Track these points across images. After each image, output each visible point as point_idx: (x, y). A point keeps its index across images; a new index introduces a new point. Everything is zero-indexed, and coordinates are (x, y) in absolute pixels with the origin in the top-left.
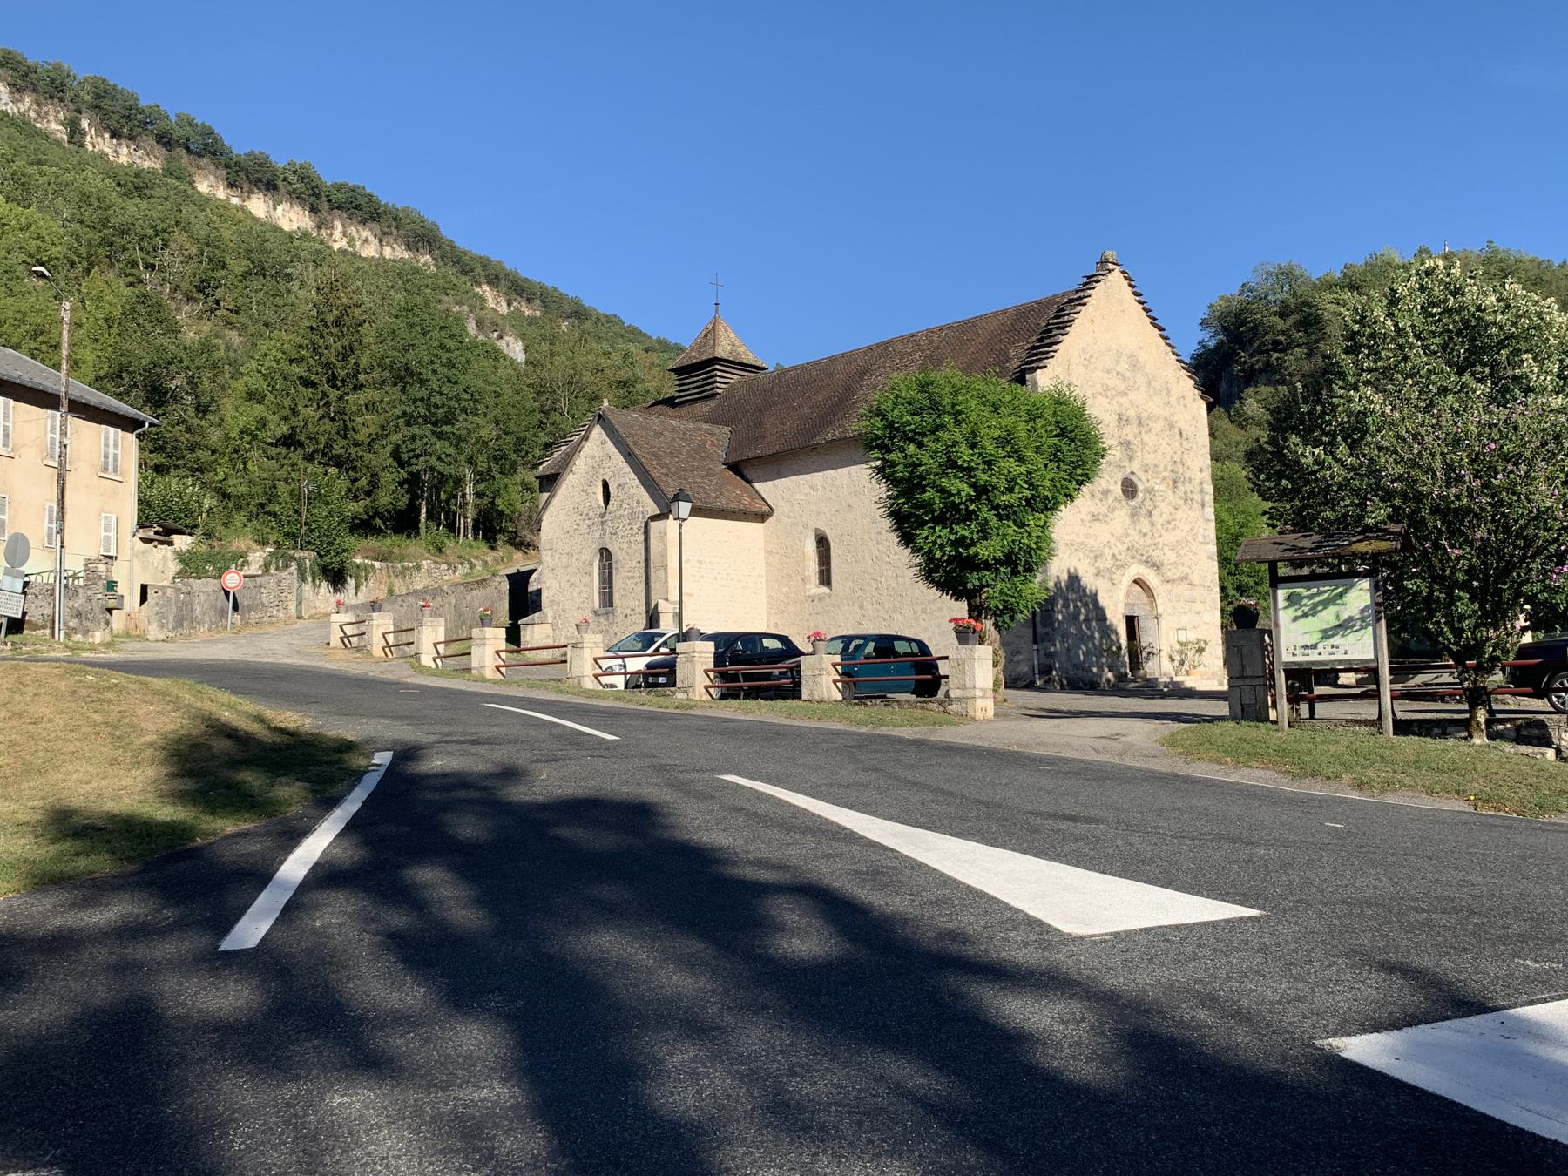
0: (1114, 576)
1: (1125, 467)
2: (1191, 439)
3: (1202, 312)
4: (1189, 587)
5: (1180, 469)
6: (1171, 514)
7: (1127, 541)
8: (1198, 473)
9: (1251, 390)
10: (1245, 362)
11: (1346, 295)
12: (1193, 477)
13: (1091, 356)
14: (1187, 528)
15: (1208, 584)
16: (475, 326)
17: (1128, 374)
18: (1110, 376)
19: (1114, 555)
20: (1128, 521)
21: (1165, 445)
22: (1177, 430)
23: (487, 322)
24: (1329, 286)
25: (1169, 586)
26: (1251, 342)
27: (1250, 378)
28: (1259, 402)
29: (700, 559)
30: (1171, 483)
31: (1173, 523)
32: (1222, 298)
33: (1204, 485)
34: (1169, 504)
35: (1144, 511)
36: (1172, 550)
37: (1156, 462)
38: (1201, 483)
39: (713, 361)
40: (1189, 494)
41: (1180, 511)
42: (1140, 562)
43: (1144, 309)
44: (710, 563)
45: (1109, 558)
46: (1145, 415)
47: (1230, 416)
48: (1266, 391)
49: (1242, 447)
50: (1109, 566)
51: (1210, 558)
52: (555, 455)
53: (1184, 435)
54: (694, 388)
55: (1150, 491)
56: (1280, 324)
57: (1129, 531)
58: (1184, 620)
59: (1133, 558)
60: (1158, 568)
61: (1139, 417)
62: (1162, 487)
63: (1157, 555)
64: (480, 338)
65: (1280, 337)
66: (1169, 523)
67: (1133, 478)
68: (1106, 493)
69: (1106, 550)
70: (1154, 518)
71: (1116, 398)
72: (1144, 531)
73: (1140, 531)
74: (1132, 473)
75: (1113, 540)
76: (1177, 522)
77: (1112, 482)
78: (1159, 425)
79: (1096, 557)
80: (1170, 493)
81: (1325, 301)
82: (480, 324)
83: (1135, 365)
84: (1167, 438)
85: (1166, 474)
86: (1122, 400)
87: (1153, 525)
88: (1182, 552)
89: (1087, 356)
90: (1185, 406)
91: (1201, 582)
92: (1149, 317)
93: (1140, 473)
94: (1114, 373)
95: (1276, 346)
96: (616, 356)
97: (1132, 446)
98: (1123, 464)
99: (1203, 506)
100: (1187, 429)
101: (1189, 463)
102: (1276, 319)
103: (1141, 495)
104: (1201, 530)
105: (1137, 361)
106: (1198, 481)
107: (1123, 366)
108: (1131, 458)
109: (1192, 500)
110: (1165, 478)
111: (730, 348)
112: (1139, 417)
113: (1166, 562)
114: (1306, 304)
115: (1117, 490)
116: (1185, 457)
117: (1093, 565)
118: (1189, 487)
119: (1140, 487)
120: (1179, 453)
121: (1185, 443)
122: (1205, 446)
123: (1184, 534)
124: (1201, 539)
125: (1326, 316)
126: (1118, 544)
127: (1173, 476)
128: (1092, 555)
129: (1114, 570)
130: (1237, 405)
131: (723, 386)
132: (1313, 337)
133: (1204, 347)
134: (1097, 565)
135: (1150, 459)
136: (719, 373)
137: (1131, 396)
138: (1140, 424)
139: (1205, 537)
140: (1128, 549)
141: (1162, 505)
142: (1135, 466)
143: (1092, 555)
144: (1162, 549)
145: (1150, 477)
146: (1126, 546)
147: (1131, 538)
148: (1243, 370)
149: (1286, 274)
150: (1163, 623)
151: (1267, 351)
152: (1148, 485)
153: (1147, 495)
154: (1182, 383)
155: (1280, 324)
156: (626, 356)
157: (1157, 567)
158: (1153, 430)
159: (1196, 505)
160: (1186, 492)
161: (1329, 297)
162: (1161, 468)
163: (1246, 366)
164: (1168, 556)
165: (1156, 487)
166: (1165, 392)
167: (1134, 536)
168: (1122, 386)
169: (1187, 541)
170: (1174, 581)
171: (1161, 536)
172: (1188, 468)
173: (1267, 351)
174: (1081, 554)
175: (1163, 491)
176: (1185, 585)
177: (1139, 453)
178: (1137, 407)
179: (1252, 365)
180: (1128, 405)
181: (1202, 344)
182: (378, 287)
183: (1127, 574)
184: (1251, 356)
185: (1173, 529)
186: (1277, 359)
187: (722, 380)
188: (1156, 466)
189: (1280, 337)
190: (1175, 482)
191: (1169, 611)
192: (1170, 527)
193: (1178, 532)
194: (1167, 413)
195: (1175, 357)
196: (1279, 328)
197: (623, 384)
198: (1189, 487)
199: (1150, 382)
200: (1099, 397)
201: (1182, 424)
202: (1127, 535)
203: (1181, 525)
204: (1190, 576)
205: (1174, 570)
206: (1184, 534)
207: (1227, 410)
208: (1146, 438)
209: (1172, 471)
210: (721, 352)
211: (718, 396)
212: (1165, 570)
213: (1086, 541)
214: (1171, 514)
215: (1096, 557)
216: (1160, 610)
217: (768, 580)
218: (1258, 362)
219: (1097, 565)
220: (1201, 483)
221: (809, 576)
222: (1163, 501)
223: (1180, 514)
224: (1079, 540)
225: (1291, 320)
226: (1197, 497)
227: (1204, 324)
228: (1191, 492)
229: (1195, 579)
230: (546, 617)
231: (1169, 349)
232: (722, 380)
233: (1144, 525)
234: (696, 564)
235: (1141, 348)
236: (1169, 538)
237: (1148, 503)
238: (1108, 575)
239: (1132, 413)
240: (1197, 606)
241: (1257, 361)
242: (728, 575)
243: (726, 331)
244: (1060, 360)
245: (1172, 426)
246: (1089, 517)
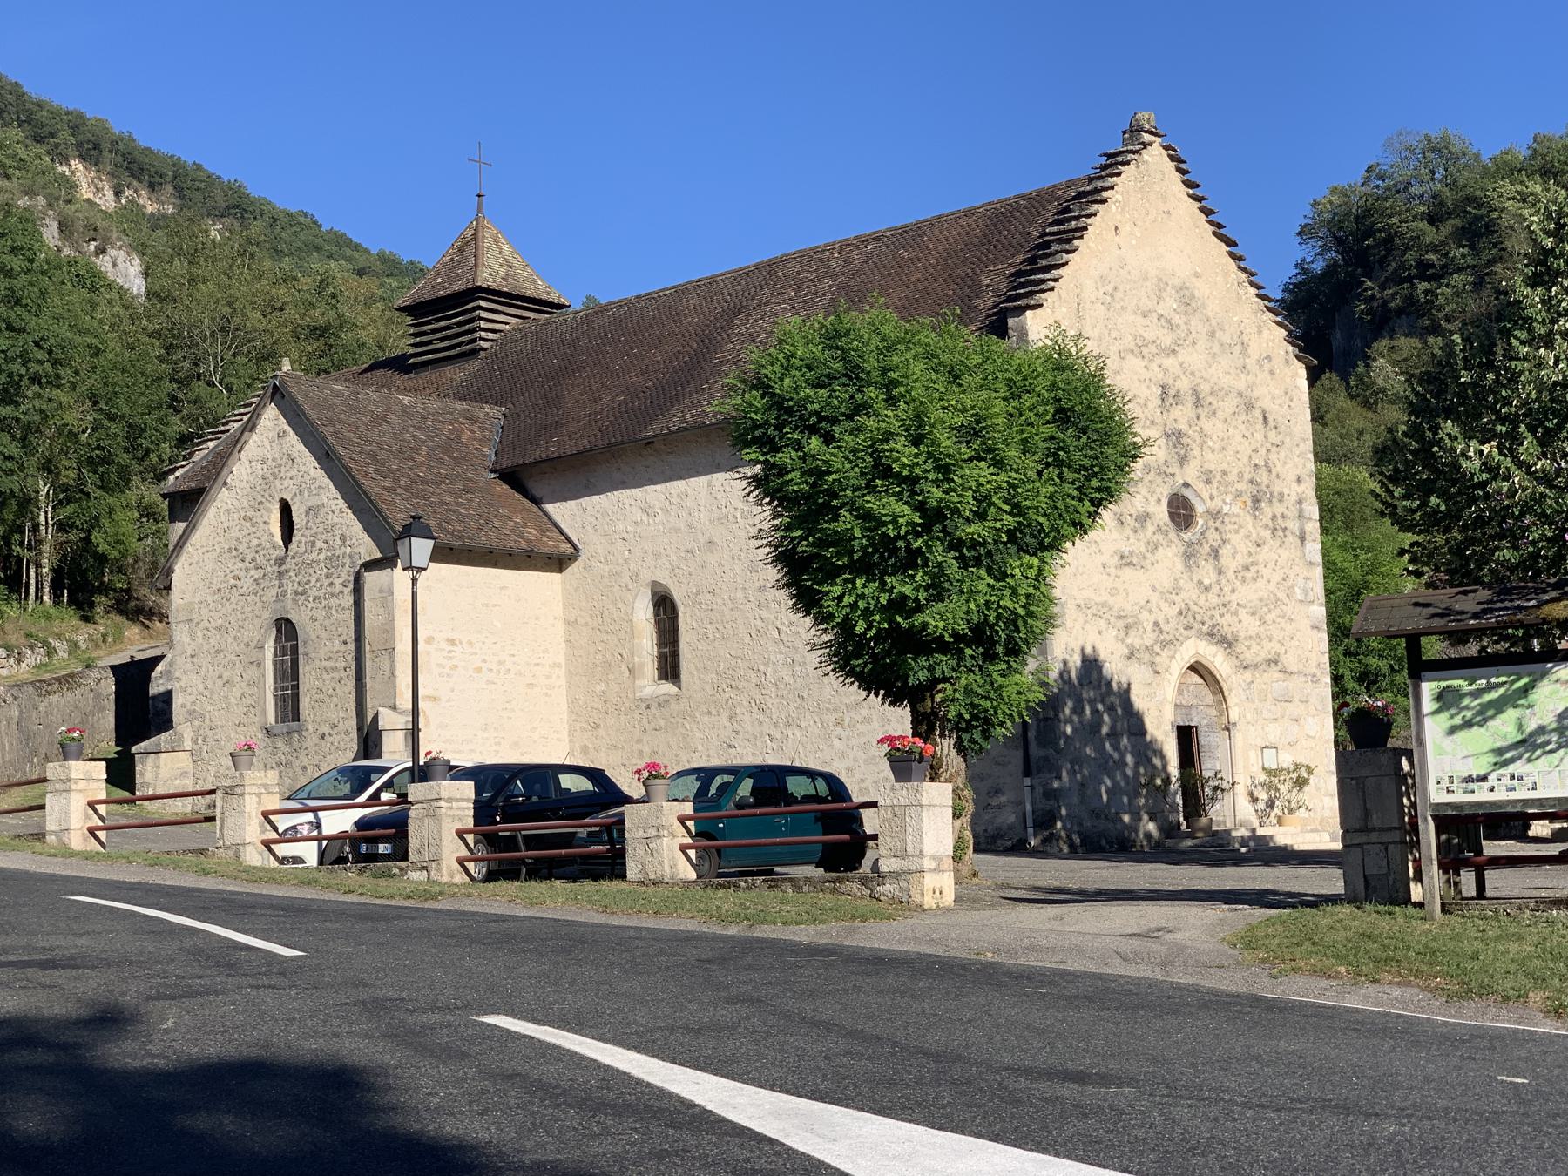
0: (1157, 659)
1: (1173, 475)
2: (1282, 429)
3: (1301, 214)
4: (1281, 675)
5: (1263, 478)
6: (1250, 554)
7: (1177, 599)
8: (1294, 485)
9: (1383, 344)
10: (1373, 297)
12: (1286, 491)
13: (1115, 289)
14: (1277, 577)
15: (1314, 670)
16: (56, 231)
17: (1177, 319)
18: (1146, 322)
19: (1157, 624)
20: (1179, 565)
21: (1239, 438)
22: (1258, 414)
23: (79, 225)
24: (1507, 169)
25: (1248, 675)
26: (1382, 263)
27: (1382, 323)
28: (1395, 363)
29: (450, 636)
30: (1249, 503)
31: (1253, 569)
32: (1334, 190)
33: (1305, 505)
34: (1248, 537)
35: (1206, 549)
36: (1253, 614)
37: (1224, 466)
38: (1300, 502)
39: (475, 292)
40: (1280, 521)
41: (1265, 548)
42: (1200, 635)
43: (1202, 209)
44: (470, 643)
45: (1149, 628)
46: (1205, 388)
47: (1348, 388)
48: (1407, 345)
50: (1148, 642)
51: (1316, 627)
52: (197, 457)
53: (1270, 419)
54: (442, 340)
55: (1215, 515)
56: (1431, 234)
57: (1181, 583)
58: (1274, 733)
59: (1188, 628)
60: (1230, 645)
61: (1195, 392)
62: (1236, 509)
63: (1227, 623)
64: (66, 252)
66: (1247, 568)
67: (1187, 493)
68: (1143, 518)
69: (1144, 616)
70: (1223, 561)
71: (1158, 360)
72: (1206, 582)
73: (1200, 583)
74: (1186, 485)
75: (1154, 598)
76: (1261, 568)
77: (1153, 501)
78: (1227, 406)
79: (1127, 627)
80: (1249, 519)
82: (65, 227)
83: (1188, 302)
84: (1242, 427)
85: (1240, 486)
86: (1169, 362)
87: (1220, 573)
88: (1269, 618)
89: (1109, 289)
90: (1272, 373)
91: (1301, 667)
92: (1211, 223)
93: (1199, 485)
94: (1155, 316)
95: (1424, 271)
96: (306, 283)
97: (1185, 440)
98: (1169, 471)
99: (1303, 539)
100: (1276, 411)
101: (1278, 468)
103: (1201, 522)
104: (1300, 581)
105: (1193, 296)
106: (1294, 498)
107: (1169, 305)
108: (1183, 460)
109: (1284, 530)
110: (1239, 494)
111: (502, 270)
112: (1195, 392)
113: (1242, 634)
114: (1471, 200)
115: (1161, 513)
116: (1273, 457)
117: (1123, 641)
118: (1279, 509)
119: (1200, 508)
120: (1263, 451)
121: (1272, 434)
122: (1304, 440)
123: (1272, 587)
124: (1299, 594)
125: (1506, 221)
126: (1164, 605)
127: (1253, 489)
128: (1121, 624)
129: (1157, 649)
130: (1361, 369)
131: (491, 336)
132: (1485, 256)
133: (1305, 271)
134: (1129, 641)
135: (1214, 461)
136: (484, 314)
137: (1183, 355)
138: (1198, 403)
139: (1306, 592)
140: (1180, 613)
141: (1236, 539)
142: (1191, 473)
143: (1121, 624)
144: (1236, 613)
145: (1215, 492)
146: (1176, 609)
147: (1183, 595)
148: (1370, 311)
149: (1439, 150)
150: (1238, 735)
151: (1410, 279)
152: (1212, 505)
153: (1211, 523)
154: (1265, 333)
155: (1431, 234)
156: (324, 284)
157: (1227, 643)
158: (1219, 413)
159: (1290, 539)
160: (1274, 517)
161: (1508, 188)
162: (1232, 477)
163: (1375, 304)
164: (1247, 625)
165: (1226, 509)
166: (1238, 349)
167: (1190, 592)
168: (1167, 340)
169: (1278, 600)
170: (1256, 666)
171: (1233, 591)
172: (1278, 476)
173: (1410, 279)
174: (1102, 623)
175: (1238, 516)
176: (1274, 673)
177: (1197, 452)
178: (1192, 374)
179: (1385, 303)
180: (1177, 370)
183: (1178, 656)
184: (1383, 287)
185: (1255, 580)
186: (1426, 292)
187: (490, 326)
188: (1224, 473)
190: (1256, 500)
191: (1249, 716)
192: (1249, 575)
193: (1261, 583)
194: (1241, 383)
195: (1253, 291)
196: (1428, 240)
197: (319, 332)
198: (1279, 509)
199: (1213, 334)
200: (1130, 357)
201: (1266, 403)
202: (1177, 589)
203: (1266, 572)
204: (1283, 658)
205: (1255, 648)
206: (1272, 587)
207: (1345, 378)
208: (1207, 424)
209: (1251, 482)
210: (486, 279)
211: (482, 354)
212: (1240, 648)
213: (1111, 601)
214: (1250, 554)
215: (1127, 627)
216: (1234, 714)
217: (570, 673)
218: (1395, 297)
219: (1129, 641)
220: (1300, 502)
221: (642, 665)
222: (1237, 532)
223: (1264, 554)
224: (1099, 600)
225: (1447, 228)
226: (1293, 525)
227: (1305, 233)
228: (1283, 516)
229: (1290, 662)
230: (181, 739)
231: (1244, 276)
232: (490, 326)
233: (1207, 573)
234: (444, 645)
235: (1197, 275)
236: (1247, 594)
237: (1212, 536)
238: (1146, 657)
239: (1184, 384)
240: (1294, 709)
241: (1393, 296)
242: (500, 663)
243: (496, 241)
244: (1063, 293)
245: (1250, 407)
246: (1117, 558)
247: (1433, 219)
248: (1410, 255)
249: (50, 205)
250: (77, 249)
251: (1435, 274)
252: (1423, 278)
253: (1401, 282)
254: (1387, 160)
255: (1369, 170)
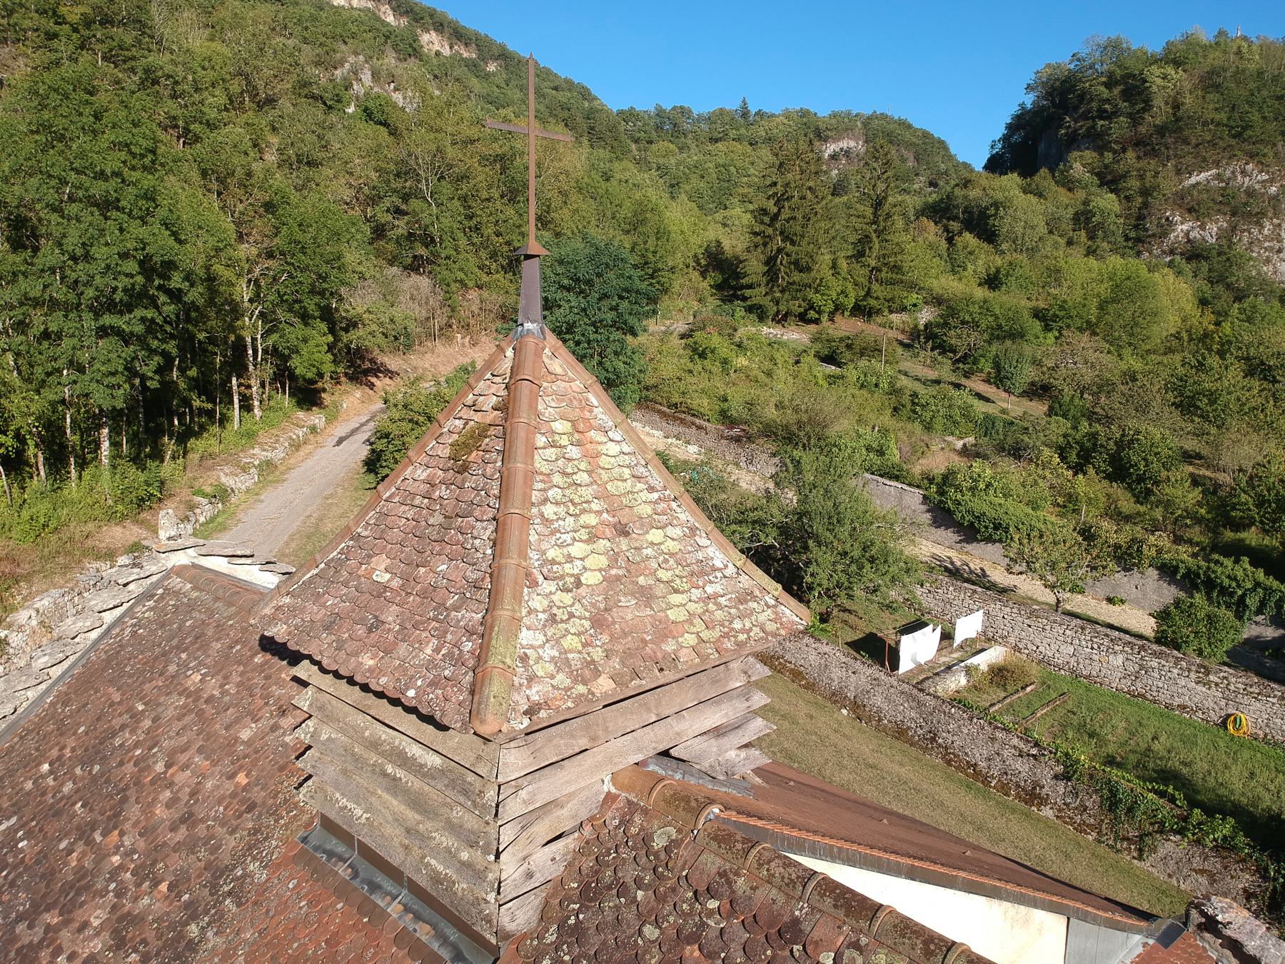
3: (1030, 78)
9: (1075, 154)
10: (1070, 126)
11: (1170, 70)
16: (370, 77)
23: (384, 74)
24: (1155, 61)
26: (1076, 108)
27: (1073, 142)
32: (1048, 66)
47: (1054, 177)
48: (1089, 155)
49: (1071, 211)
56: (1105, 93)
64: (376, 89)
65: (1107, 106)
81: (1155, 76)
82: (376, 76)
95: (1102, 114)
102: (1102, 88)
125: (1155, 88)
130: (1061, 167)
132: (1137, 107)
148: (1066, 134)
149: (1114, 46)
155: (1105, 93)
161: (1155, 70)
163: (1070, 130)
179: (1076, 130)
181: (1022, 106)
182: (254, 35)
184: (1076, 121)
186: (1102, 126)
189: (1107, 106)
196: (1105, 96)
197: (500, 158)
207: (1052, 170)
225: (1116, 91)
241: (1081, 127)
247: (1108, 85)
248: (1094, 105)
249: (366, 62)
250: (382, 88)
251: (1109, 116)
252: (1101, 118)
253: (1087, 119)
254: (1084, 52)
255: (1074, 55)
